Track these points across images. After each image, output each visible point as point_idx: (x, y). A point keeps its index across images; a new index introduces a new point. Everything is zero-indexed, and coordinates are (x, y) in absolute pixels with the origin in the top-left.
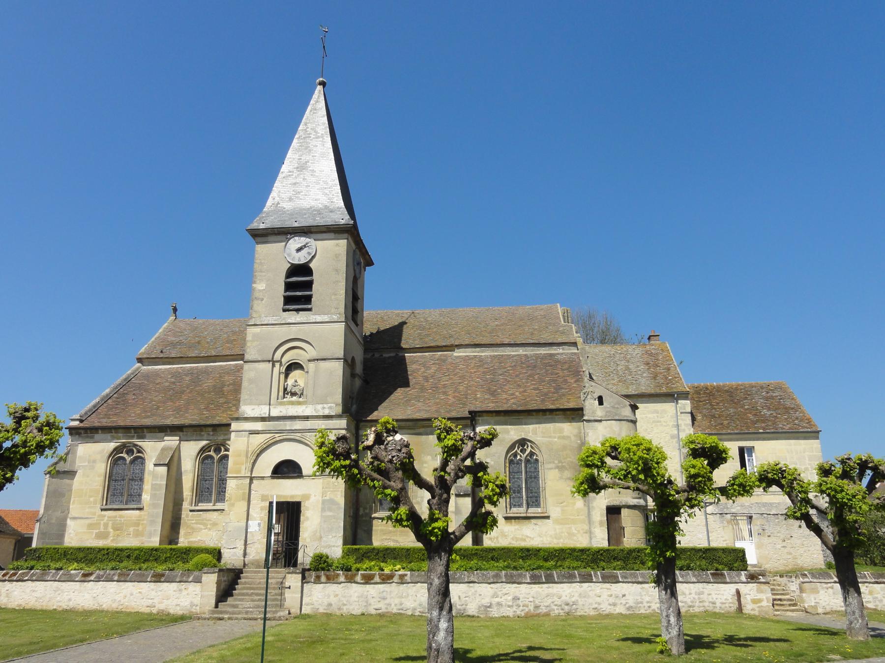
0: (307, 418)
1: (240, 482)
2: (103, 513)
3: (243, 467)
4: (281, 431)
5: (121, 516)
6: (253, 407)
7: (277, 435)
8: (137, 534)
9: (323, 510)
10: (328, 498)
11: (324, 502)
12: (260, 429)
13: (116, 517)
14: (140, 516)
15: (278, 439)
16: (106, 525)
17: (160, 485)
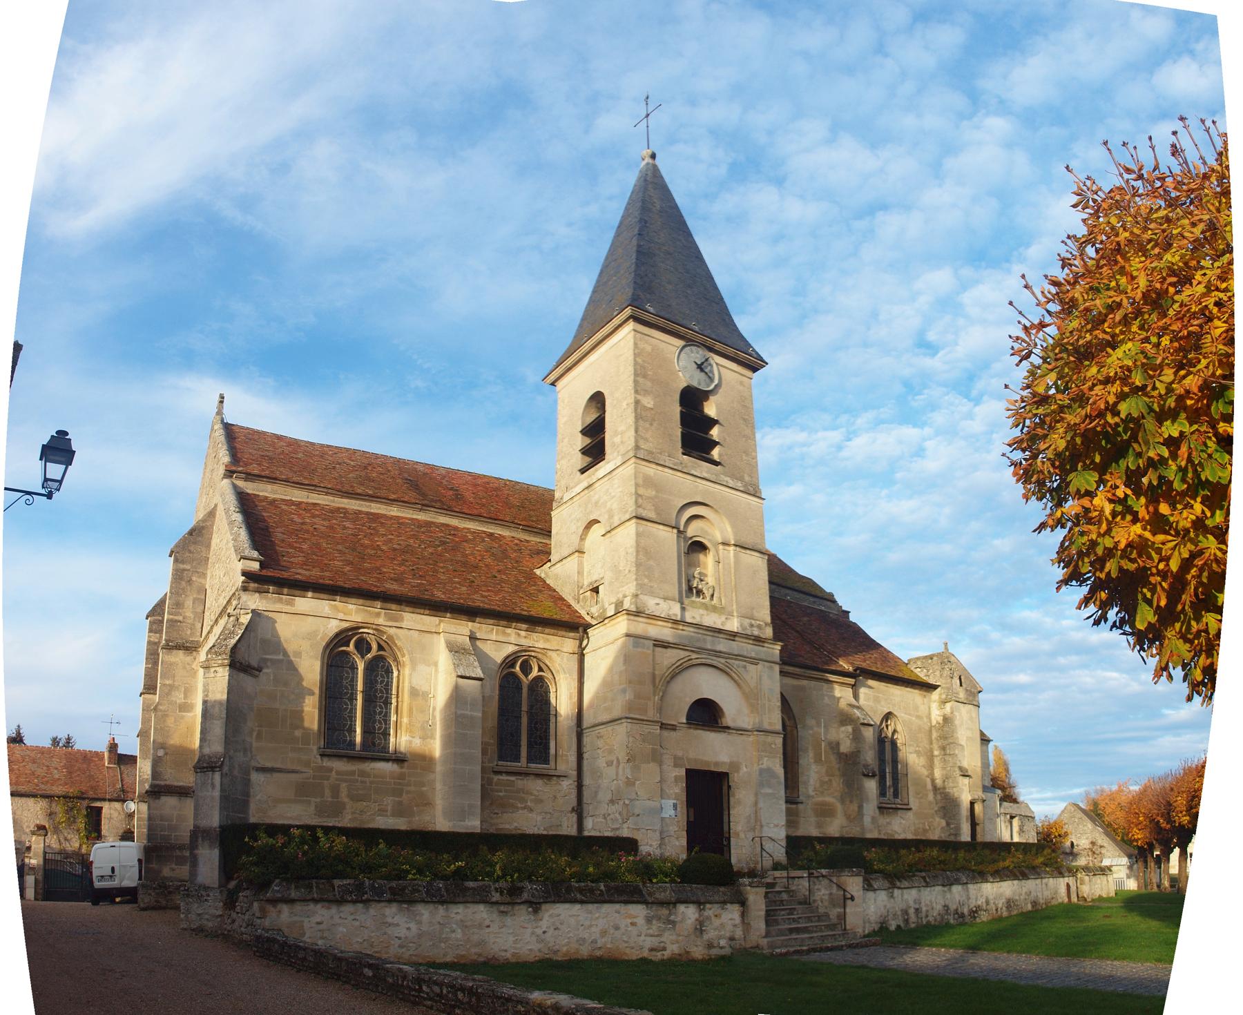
0: (733, 636)
1: (647, 729)
2: (327, 763)
3: (650, 704)
4: (699, 650)
5: (363, 773)
6: (657, 601)
7: (694, 656)
8: (400, 811)
9: (761, 785)
10: (764, 766)
11: (761, 771)
12: (670, 639)
13: (353, 773)
14: (402, 776)
15: (695, 662)
16: (335, 791)
17: (472, 717)
